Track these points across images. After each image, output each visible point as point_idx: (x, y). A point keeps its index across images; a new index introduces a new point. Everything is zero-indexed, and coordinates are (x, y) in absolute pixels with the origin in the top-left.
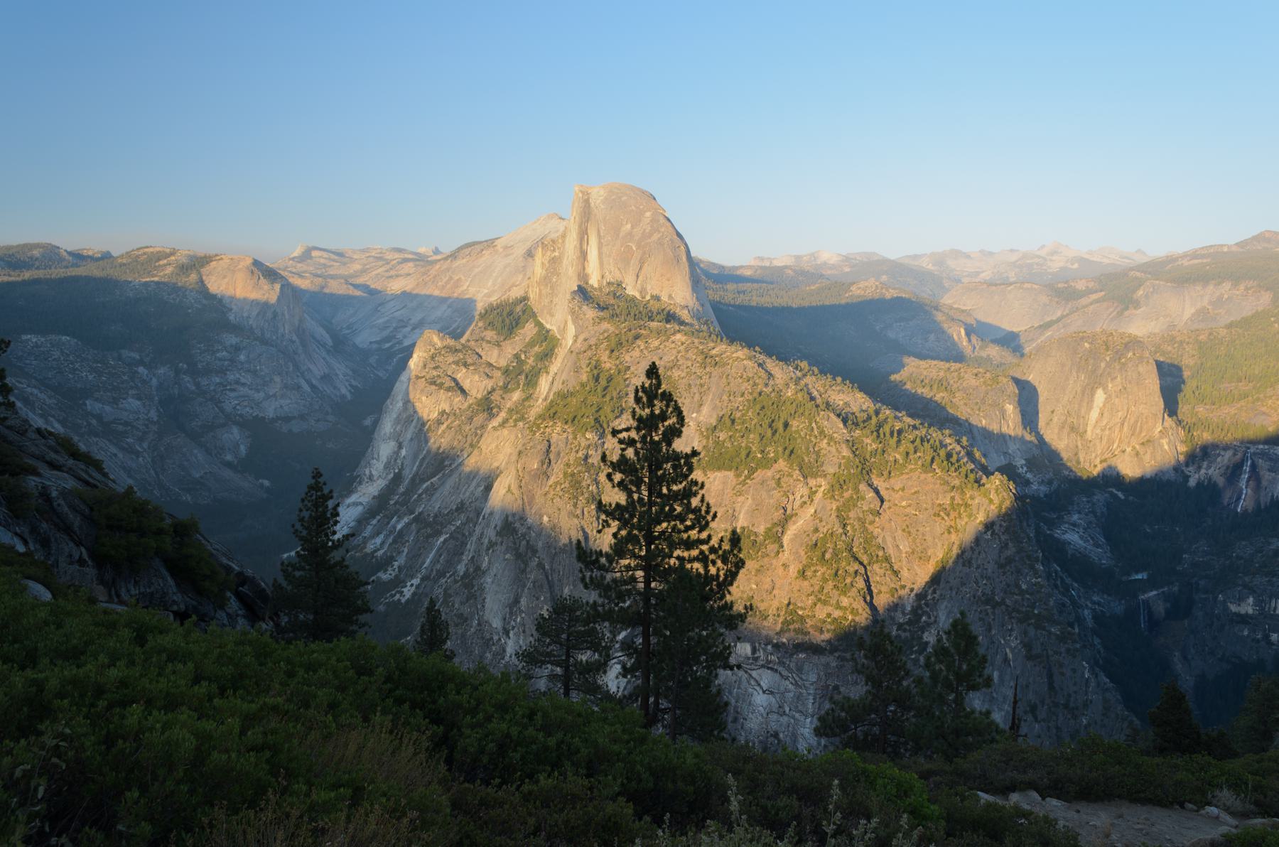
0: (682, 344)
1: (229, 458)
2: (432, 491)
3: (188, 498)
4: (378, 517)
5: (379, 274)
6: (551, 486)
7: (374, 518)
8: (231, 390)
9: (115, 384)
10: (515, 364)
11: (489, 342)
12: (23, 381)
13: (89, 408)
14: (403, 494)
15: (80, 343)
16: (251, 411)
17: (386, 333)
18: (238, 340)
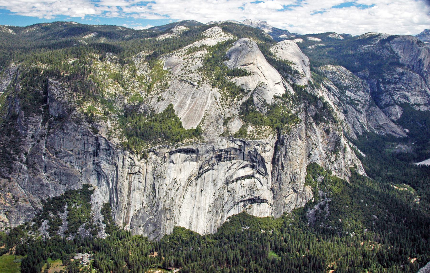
1: (393, 118)
3: (376, 132)
8: (397, 91)
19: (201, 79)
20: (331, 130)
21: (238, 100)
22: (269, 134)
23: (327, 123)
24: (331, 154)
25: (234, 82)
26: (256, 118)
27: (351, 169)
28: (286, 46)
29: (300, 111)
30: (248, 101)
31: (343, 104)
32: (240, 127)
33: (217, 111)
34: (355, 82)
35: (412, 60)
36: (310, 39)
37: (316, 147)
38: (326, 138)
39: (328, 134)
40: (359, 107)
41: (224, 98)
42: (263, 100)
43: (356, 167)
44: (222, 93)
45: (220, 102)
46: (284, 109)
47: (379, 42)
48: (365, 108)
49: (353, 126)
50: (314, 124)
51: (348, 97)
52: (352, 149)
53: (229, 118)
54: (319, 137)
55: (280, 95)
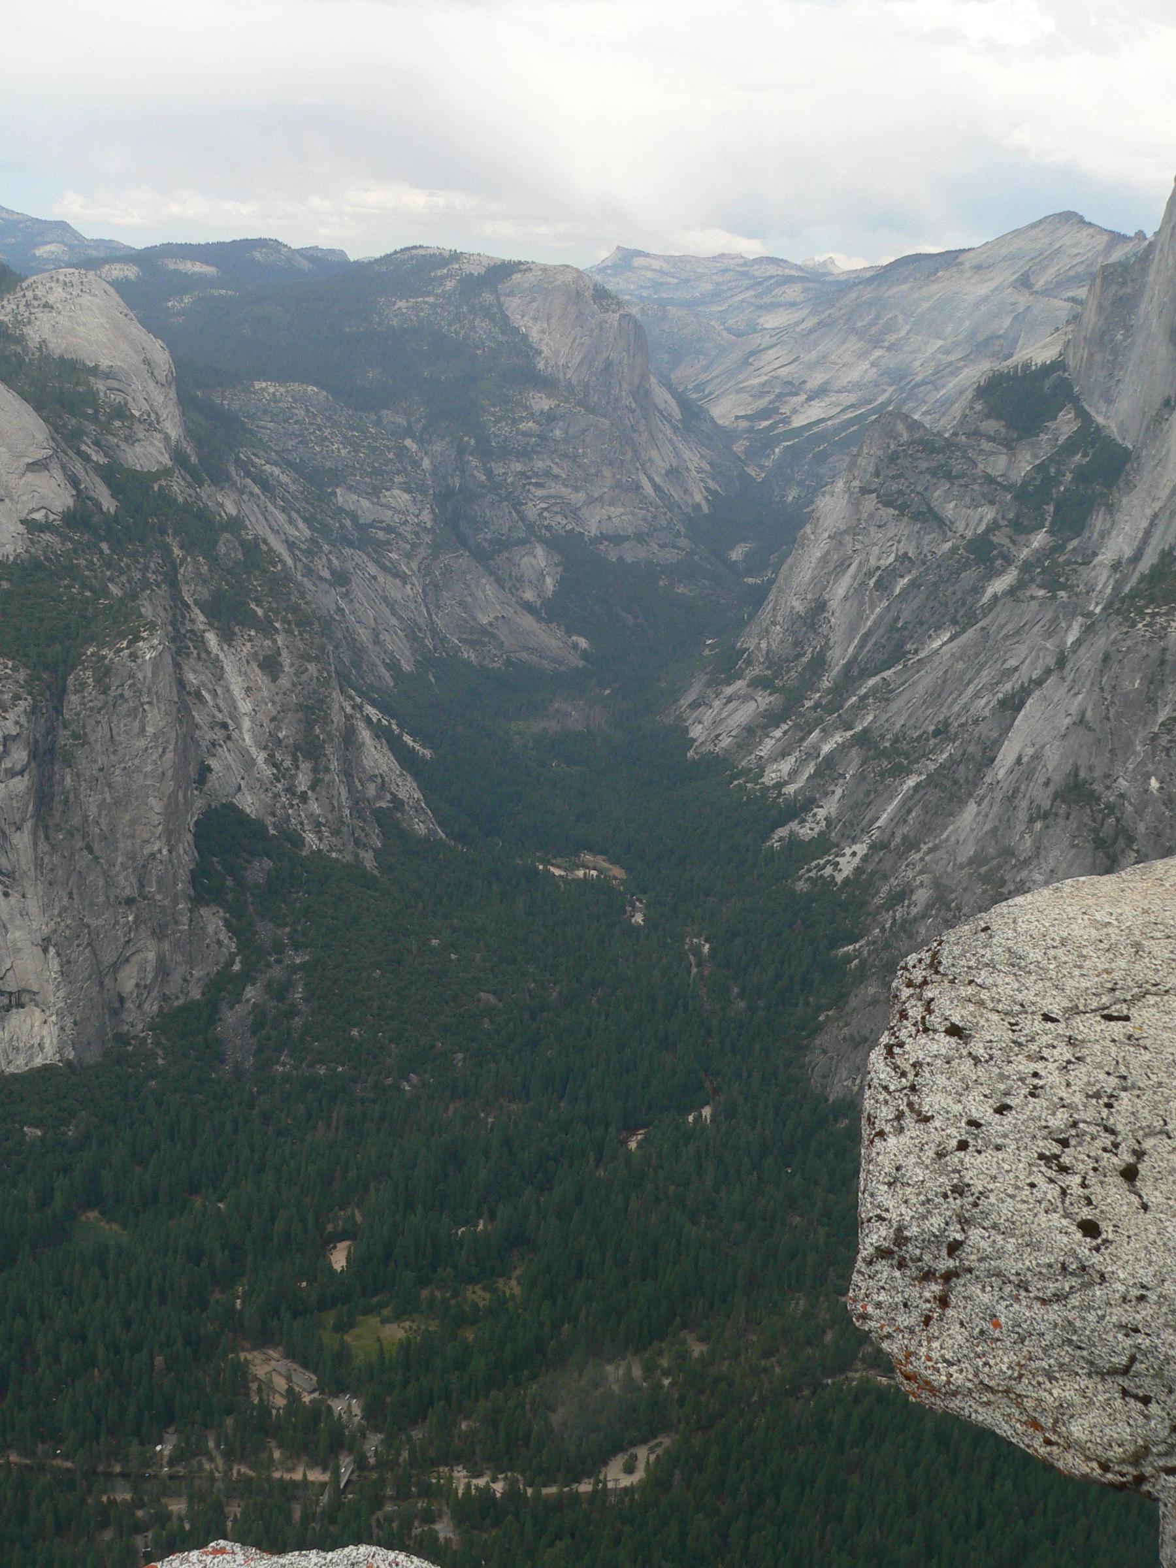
1: (529, 595)
2: (885, 694)
3: (469, 654)
4: (785, 727)
5: (743, 301)
6: (1162, 724)
8: (537, 485)
9: (376, 465)
10: (1037, 483)
11: (991, 439)
12: (261, 453)
13: (340, 499)
14: (829, 691)
15: (330, 398)
16: (565, 522)
17: (762, 403)
18: (552, 403)
20: (286, 660)
22: (17, 697)
23: (267, 629)
24: (295, 760)
27: (381, 817)
29: (145, 584)
31: (326, 547)
35: (582, 362)
38: (265, 693)
39: (274, 679)
40: (392, 555)
43: (397, 803)
48: (420, 557)
49: (377, 636)
50: (211, 638)
51: (347, 513)
52: (380, 732)
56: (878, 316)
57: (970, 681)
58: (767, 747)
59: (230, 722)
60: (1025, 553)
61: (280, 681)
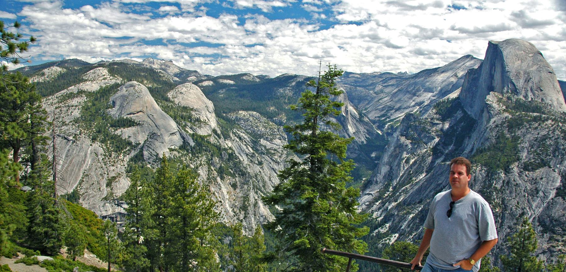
0: (552, 125)
4: (380, 202)
7: (377, 201)
11: (438, 119)
14: (391, 191)
17: (383, 113)
19: (78, 132)
20: (238, 184)
21: (124, 156)
23: (233, 176)
24: (240, 211)
25: (119, 135)
26: (147, 175)
28: (186, 90)
29: (201, 165)
30: (136, 156)
32: (127, 188)
33: (99, 170)
34: (270, 129)
36: (221, 81)
37: (222, 205)
38: (233, 193)
39: (235, 189)
40: (276, 157)
41: (107, 154)
42: (156, 154)
44: (105, 147)
45: (103, 159)
46: (181, 162)
47: (294, 86)
48: (283, 157)
49: (270, 179)
51: (263, 146)
53: (113, 177)
54: (225, 193)
55: (176, 147)
56: (415, 87)
57: (429, 187)
58: (375, 207)
59: (222, 201)
60: (447, 151)
61: (236, 190)
